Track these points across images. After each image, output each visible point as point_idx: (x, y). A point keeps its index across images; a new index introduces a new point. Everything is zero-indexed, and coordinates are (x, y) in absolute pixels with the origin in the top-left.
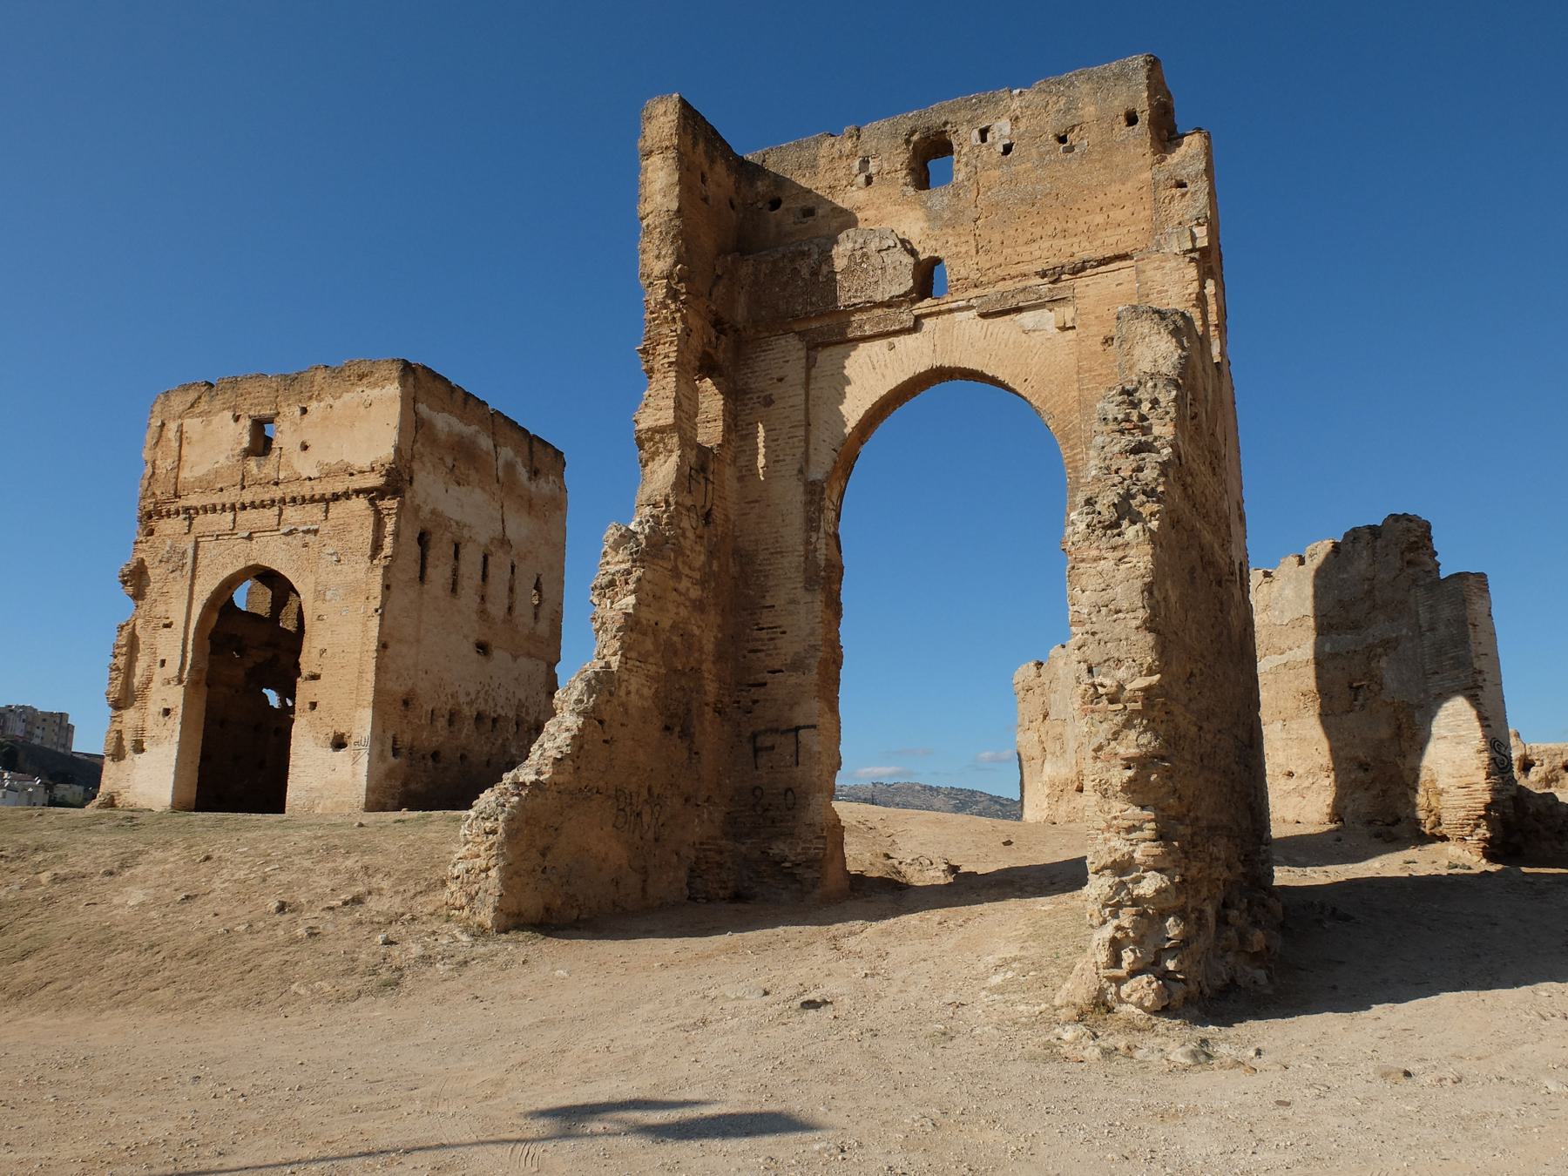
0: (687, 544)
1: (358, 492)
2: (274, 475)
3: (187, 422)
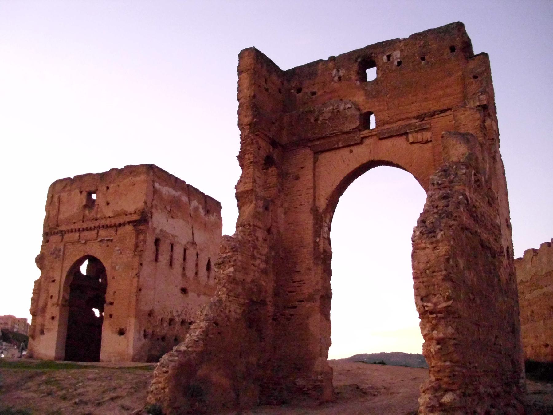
0: (259, 243)
1: (129, 222)
2: (95, 216)
3: (62, 194)
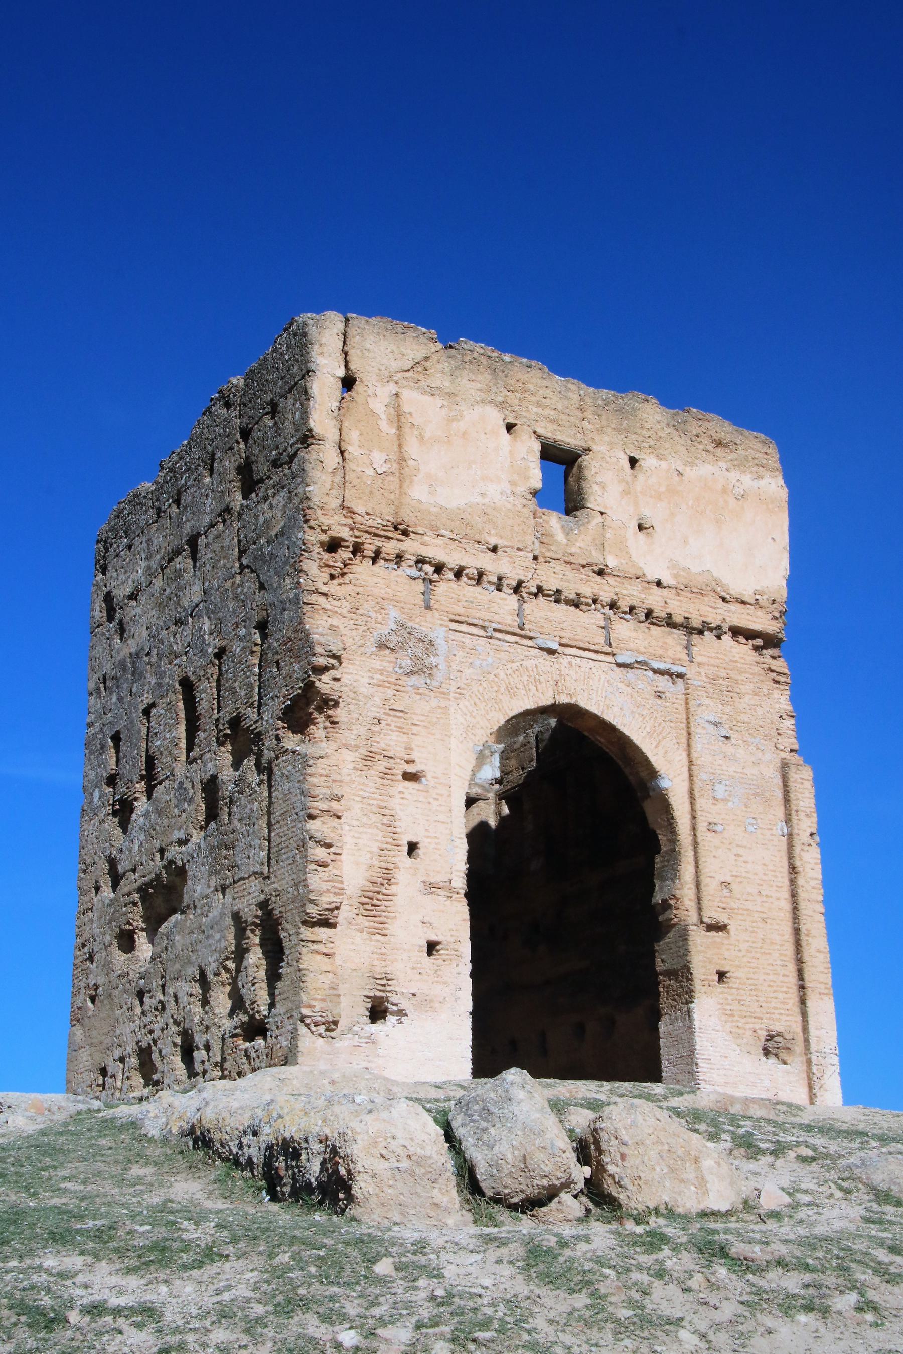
1: (737, 632)
2: (596, 557)
